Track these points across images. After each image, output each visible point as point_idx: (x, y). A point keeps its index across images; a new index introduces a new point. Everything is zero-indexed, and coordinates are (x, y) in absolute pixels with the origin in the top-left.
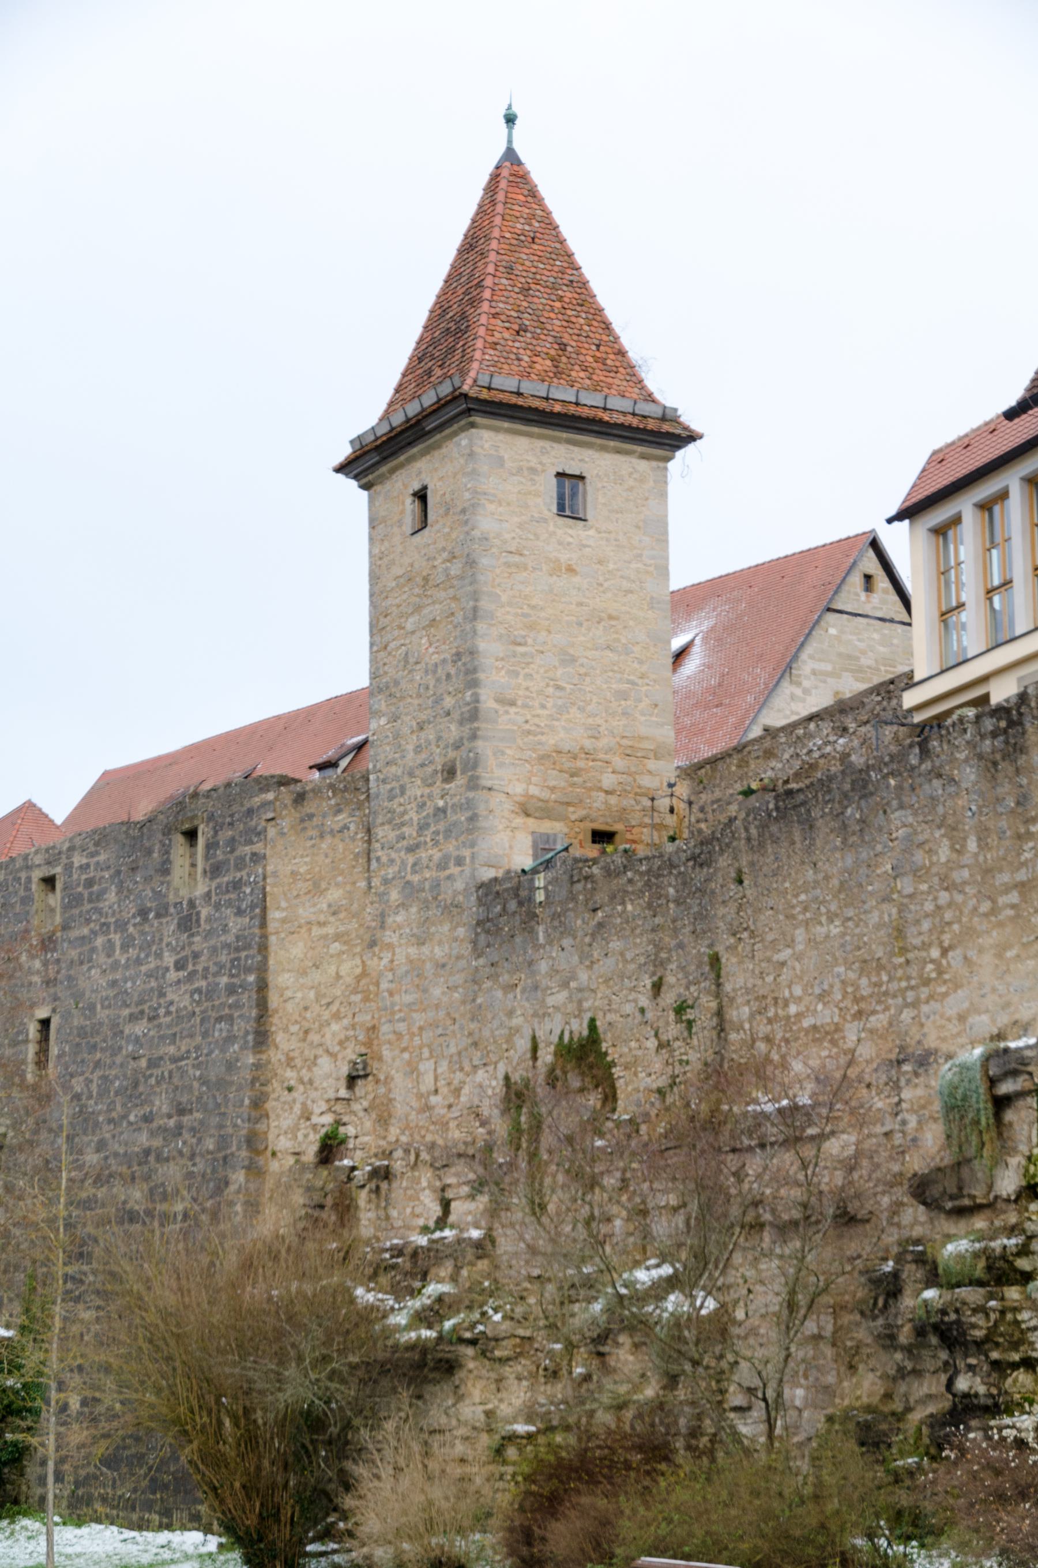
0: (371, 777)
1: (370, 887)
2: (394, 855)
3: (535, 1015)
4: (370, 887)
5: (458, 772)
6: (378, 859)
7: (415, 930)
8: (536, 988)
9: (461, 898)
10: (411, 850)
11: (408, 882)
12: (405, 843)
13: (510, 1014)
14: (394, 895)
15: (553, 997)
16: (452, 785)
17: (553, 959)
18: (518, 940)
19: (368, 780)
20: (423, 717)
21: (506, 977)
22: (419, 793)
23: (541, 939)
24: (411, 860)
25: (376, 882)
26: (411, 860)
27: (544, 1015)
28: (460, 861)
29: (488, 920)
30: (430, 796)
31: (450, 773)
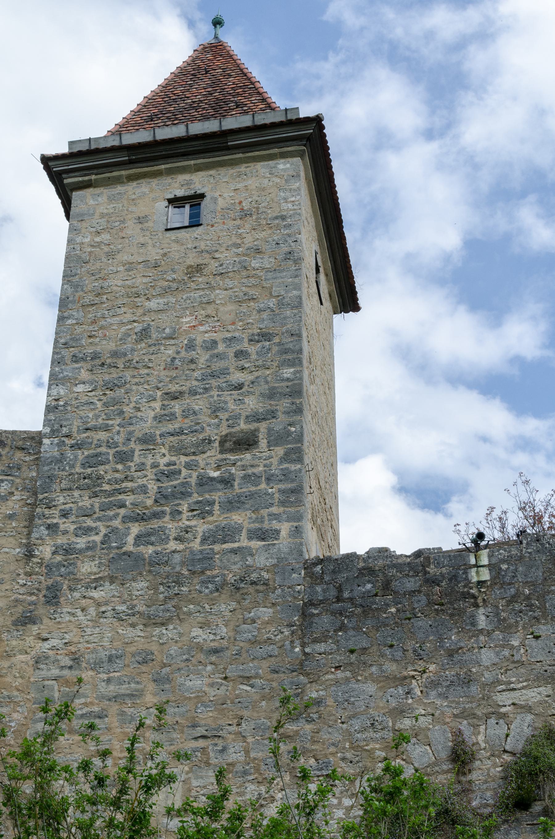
0: (46, 441)
1: (29, 555)
2: (89, 522)
3: (463, 715)
4: (29, 555)
5: (263, 443)
6: (52, 528)
7: (141, 608)
8: (468, 681)
9: (266, 575)
10: (140, 518)
11: (128, 554)
12: (122, 511)
13: (400, 712)
14: (87, 568)
15: (513, 694)
16: (248, 456)
17: (512, 647)
18: (422, 623)
19: (40, 443)
20: (174, 388)
21: (391, 668)
22: (163, 461)
23: (482, 621)
24: (135, 529)
25: (45, 551)
26: (135, 529)
27: (488, 716)
28: (261, 535)
29: (339, 599)
30: (188, 466)
31: (246, 443)
